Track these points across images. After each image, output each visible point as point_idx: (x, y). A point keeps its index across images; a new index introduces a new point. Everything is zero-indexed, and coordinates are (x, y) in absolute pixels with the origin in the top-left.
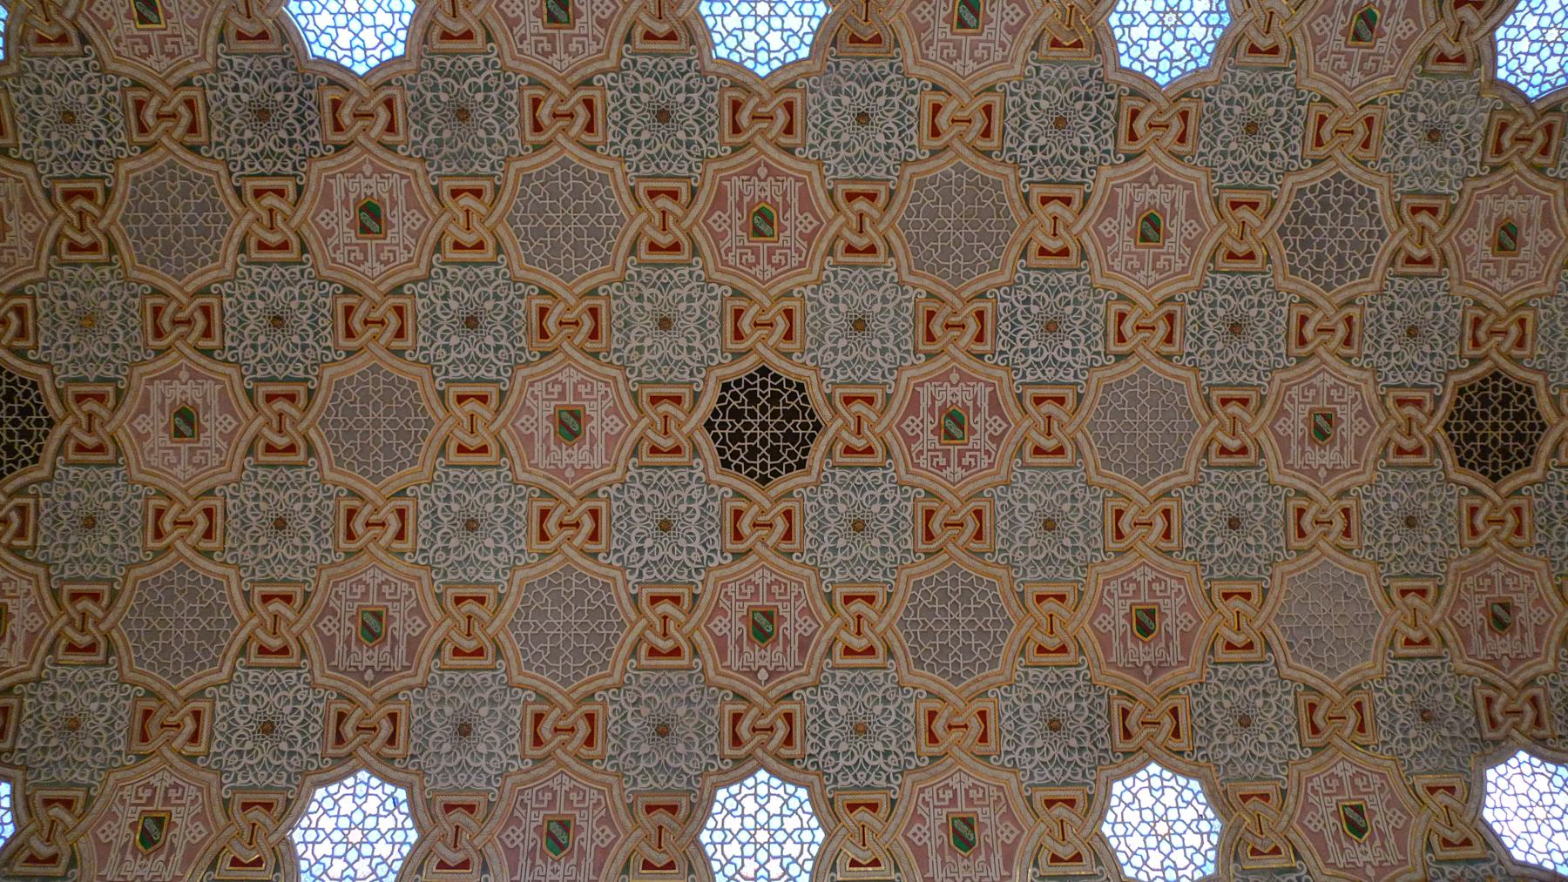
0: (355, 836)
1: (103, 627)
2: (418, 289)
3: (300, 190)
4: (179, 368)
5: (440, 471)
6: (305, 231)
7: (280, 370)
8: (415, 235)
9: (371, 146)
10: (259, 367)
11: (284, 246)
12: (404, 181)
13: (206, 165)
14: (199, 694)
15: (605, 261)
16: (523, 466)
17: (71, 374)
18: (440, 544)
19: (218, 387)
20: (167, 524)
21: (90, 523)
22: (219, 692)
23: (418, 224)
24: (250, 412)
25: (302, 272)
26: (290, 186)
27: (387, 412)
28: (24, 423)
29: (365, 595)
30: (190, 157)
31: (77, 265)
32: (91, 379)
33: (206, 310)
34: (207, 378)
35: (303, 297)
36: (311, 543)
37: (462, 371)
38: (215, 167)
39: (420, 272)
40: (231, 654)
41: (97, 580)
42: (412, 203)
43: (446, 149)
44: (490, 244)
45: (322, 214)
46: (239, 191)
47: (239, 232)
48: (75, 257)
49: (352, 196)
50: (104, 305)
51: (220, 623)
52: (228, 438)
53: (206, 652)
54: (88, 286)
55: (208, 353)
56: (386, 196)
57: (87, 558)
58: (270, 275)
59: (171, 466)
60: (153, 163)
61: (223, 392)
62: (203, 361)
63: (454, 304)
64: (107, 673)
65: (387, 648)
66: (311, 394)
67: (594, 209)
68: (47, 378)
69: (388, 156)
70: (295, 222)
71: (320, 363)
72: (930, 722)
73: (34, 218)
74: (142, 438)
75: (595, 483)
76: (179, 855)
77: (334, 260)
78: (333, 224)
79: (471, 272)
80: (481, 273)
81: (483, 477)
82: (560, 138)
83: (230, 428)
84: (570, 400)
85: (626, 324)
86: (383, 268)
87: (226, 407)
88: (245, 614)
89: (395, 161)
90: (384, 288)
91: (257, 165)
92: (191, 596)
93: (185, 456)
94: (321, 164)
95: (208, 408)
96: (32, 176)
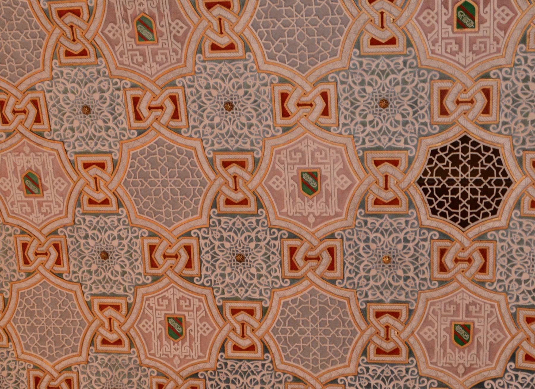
2: (142, 279)
3: (222, 349)
4: (315, 224)
5: (115, 149)
6: (221, 321)
7: (238, 222)
8: (145, 316)
9: (174, 376)
10: (254, 225)
11: (234, 312)
12: (152, 352)
13: (289, 369)
15: (23, 296)
16: (59, 154)
17: (403, 220)
18: (106, 95)
19: (284, 210)
20: (320, 104)
23: (143, 323)
24: (260, 190)
25: (223, 293)
26: (230, 352)
27: (157, 193)
28: (444, 182)
29: (155, 54)
30: (301, 374)
31: (394, 302)
32: (386, 216)
35: (223, 275)
36: (203, 91)
37: (108, 221)
38: (282, 367)
39: (141, 291)
42: (147, 338)
43: (126, 371)
44: (96, 308)
45: (208, 332)
46: (266, 349)
47: (268, 322)
48: (395, 308)
49: (187, 344)
50: (373, 272)
52: (275, 172)
54: (387, 286)
55: (292, 236)
56: (165, 342)
57: (383, 74)
58: (246, 291)
61: (281, 205)
62: (296, 230)
63: (118, 268)
65: (130, 12)
66: (214, 205)
67: (32, 329)
68: (423, 217)
69: (163, 369)
70: (227, 328)
71: (209, 227)
73: (426, 337)
74: (344, 171)
75: (10, 142)
77: (200, 300)
78: (201, 325)
79: (108, 290)
80: (101, 288)
81: (85, 146)
82: (56, 375)
83: (274, 179)
84: (35, 201)
85: (6, 252)
86: (166, 294)
89: (158, 365)
90: (166, 281)
91: (252, 367)
92: (293, 46)
93: (308, 158)
94: (208, 366)
96: (422, 366)
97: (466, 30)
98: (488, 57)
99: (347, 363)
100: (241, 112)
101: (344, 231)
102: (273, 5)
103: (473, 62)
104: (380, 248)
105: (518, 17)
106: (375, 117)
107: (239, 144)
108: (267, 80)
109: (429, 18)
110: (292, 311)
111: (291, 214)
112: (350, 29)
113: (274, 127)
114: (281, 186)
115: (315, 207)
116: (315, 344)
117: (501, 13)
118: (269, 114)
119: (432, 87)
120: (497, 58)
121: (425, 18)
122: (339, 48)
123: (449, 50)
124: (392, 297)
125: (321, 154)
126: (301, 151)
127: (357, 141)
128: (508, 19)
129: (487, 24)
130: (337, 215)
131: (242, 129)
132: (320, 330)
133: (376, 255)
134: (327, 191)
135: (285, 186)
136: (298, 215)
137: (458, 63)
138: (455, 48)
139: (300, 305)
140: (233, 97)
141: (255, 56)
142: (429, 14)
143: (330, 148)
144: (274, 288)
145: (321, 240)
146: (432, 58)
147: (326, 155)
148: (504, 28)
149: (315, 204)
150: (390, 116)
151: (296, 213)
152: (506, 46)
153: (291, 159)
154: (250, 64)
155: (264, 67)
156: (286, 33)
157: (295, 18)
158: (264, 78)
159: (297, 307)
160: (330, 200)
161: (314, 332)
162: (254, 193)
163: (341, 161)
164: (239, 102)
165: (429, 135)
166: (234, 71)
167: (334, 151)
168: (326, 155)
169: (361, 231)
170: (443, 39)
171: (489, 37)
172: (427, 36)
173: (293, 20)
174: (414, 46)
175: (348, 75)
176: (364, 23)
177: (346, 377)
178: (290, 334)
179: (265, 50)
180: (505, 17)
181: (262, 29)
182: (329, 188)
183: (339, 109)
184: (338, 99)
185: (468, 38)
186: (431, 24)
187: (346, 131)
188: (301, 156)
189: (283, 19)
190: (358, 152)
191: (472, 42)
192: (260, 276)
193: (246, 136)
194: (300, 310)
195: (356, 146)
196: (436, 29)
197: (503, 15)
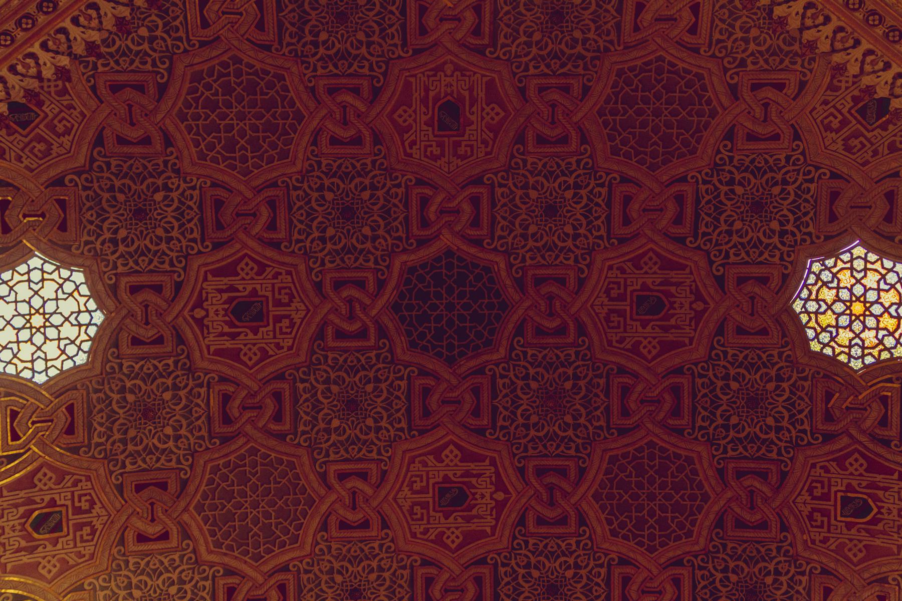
0: (37, 321)
1: (248, 428)
4: (506, 491)
13: (704, 533)
14: (186, 534)
19: (488, 530)
21: (352, 405)
22: (189, 554)
32: (495, 402)
33: (563, 521)
34: (497, 520)
40: (226, 560)
41: (296, 417)
51: (257, 546)
52: (439, 540)
53: (227, 535)
57: (317, 407)
59: (411, 484)
60: (707, 479)
61: (482, 534)
64: (202, 438)
72: (155, 485)
74: (437, 454)
76: (26, 559)
83: (449, 542)
87: (470, 537)
88: (266, 568)
95: (468, 520)
97: (265, 310)
98: (297, 285)
99: (694, 455)
100: (363, 579)
101: (515, 455)
102: (233, 536)
103: (302, 301)
104: (536, 410)
105: (249, 253)
106: (369, 416)
107: (404, 584)
108: (323, 546)
109: (250, 354)
110: (622, 525)
111: (494, 522)
112: (263, 446)
113: (383, 539)
114: (457, 532)
115: (484, 491)
116: (668, 497)
117: (245, 271)
118: (366, 545)
119: (333, 349)
120: (297, 273)
121: (250, 359)
122: (285, 458)
123: (289, 330)
124: (602, 397)
125: (416, 482)
126: (412, 507)
127: (400, 437)
128: (251, 264)
129: (258, 287)
130: (493, 463)
131: (384, 580)
132: (648, 489)
133: (546, 416)
134: (462, 476)
135: (457, 528)
136: (494, 513)
137: (303, 319)
138: (286, 322)
139: (614, 515)
140: (345, 588)
141: (293, 559)
142: (245, 354)
143: (408, 470)
144: (592, 548)
145: (527, 483)
146: (298, 349)
147: (417, 476)
148: (262, 268)
149: (479, 491)
150: (368, 397)
151: (491, 515)
152: (283, 264)
153: (422, 519)
154: (303, 566)
155: (308, 548)
156: (266, 521)
157: (249, 510)
158: (321, 550)
159: (617, 519)
160: (475, 472)
161: (651, 497)
162: (466, 568)
163: (425, 458)
164: (351, 581)
165: (391, 351)
166: (312, 586)
167: (412, 465)
168: (417, 476)
169: (515, 434)
170: (275, 337)
171: (273, 284)
172: (272, 356)
173: (251, 512)
174: (284, 370)
175: (318, 448)
176: (255, 429)
177: (714, 456)
178: (655, 529)
179: (287, 547)
180: (249, 267)
181: (262, 549)
182: (459, 473)
183: (360, 460)
184: (346, 460)
185: (274, 309)
186: (257, 352)
187: (387, 452)
188: (419, 507)
189: (250, 525)
190: (414, 436)
191: (278, 303)
192: (577, 566)
193: (394, 574)
194: (621, 515)
195: (406, 439)
196: (264, 345)
197: (247, 269)
